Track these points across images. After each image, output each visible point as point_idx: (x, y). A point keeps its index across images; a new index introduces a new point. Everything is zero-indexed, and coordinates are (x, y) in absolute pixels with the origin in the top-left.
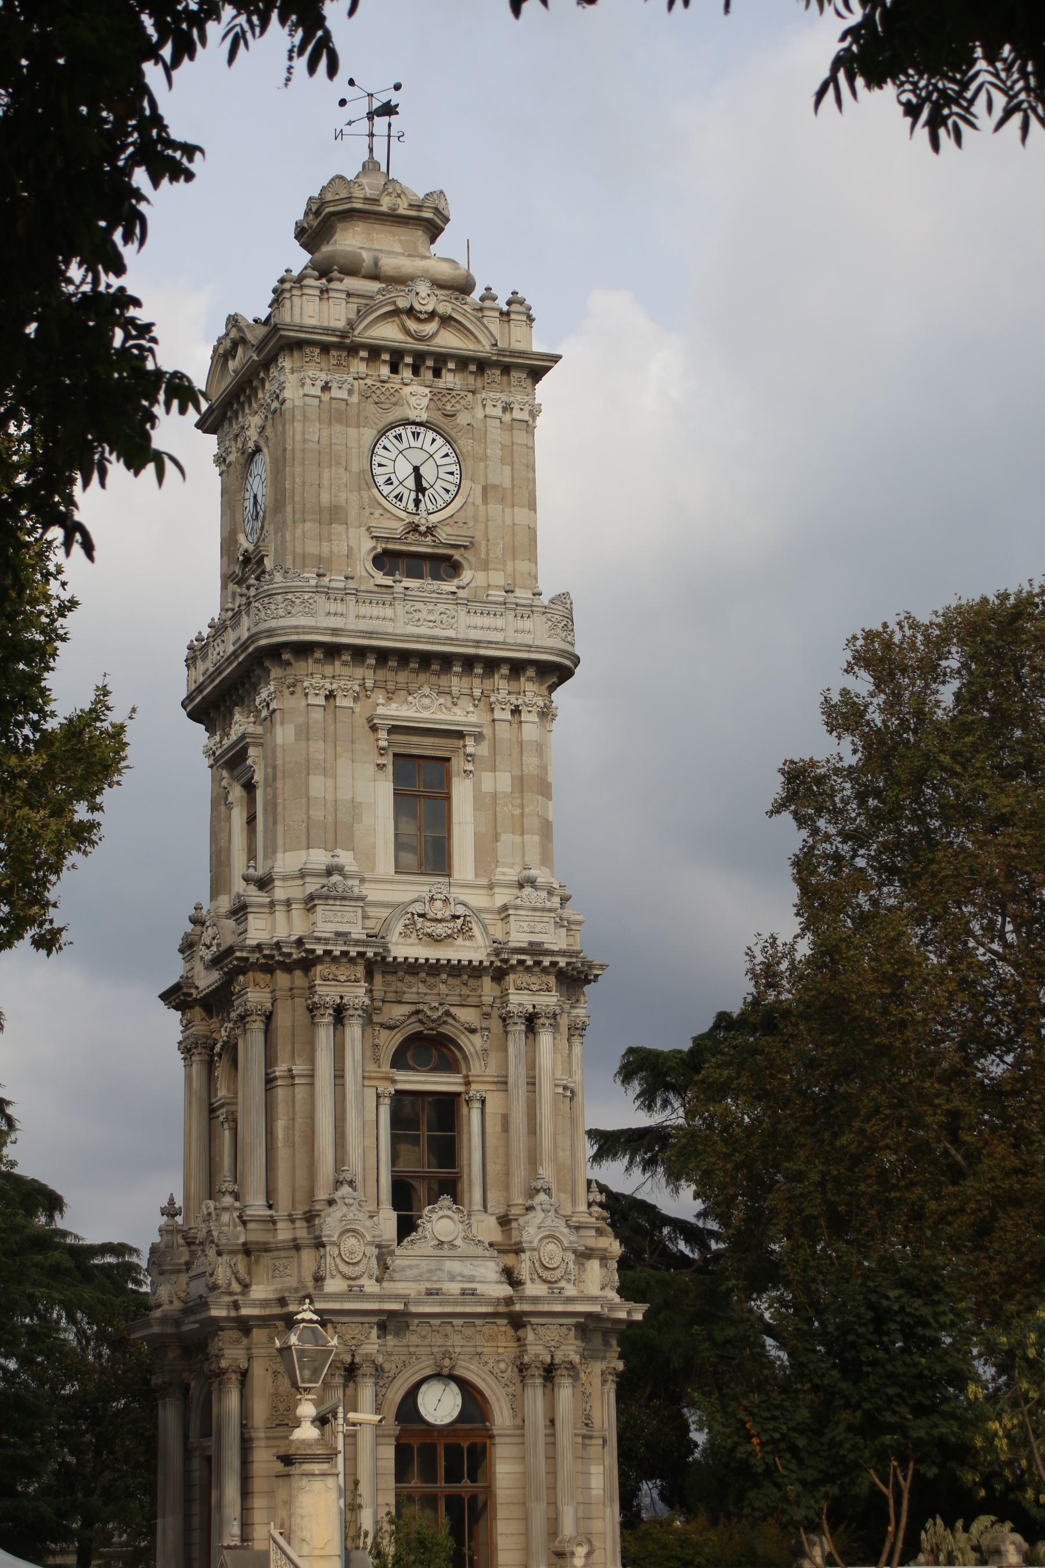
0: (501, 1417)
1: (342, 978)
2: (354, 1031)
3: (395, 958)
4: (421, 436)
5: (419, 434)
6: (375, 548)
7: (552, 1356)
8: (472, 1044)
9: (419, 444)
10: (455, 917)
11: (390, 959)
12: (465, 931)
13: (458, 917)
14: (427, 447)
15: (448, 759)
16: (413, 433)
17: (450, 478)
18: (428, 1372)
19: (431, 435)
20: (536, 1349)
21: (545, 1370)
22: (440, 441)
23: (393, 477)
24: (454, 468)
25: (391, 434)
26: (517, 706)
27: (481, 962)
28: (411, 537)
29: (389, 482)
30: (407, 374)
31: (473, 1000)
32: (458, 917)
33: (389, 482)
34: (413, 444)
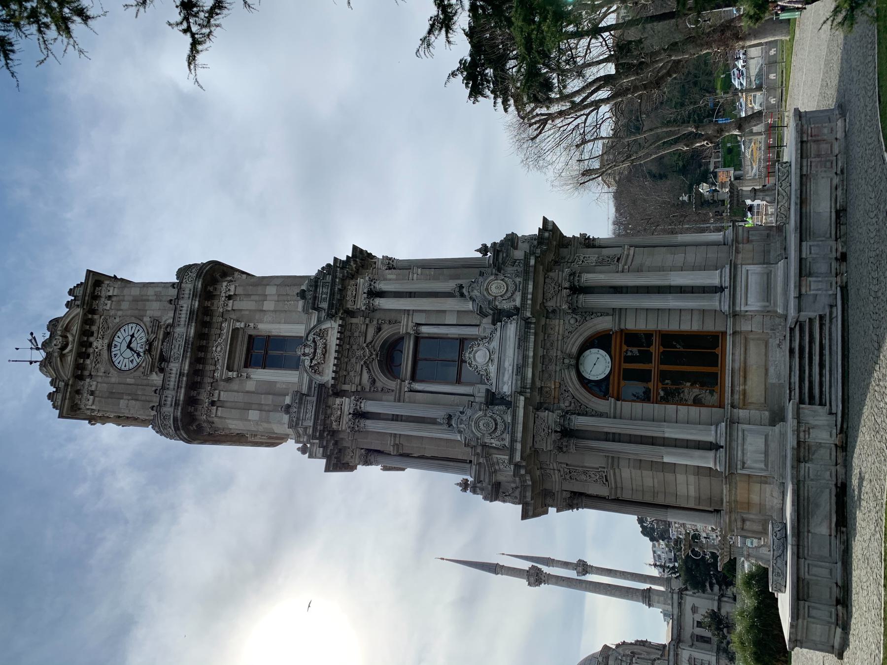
0: (604, 324)
1: (339, 413)
2: (369, 406)
3: (333, 378)
4: (116, 343)
5: (115, 345)
6: (156, 373)
7: (565, 288)
8: (387, 332)
9: (119, 344)
10: (314, 341)
11: (332, 382)
12: (322, 334)
13: (314, 338)
14: (120, 341)
15: (250, 336)
16: (115, 347)
17: (134, 328)
18: (573, 374)
19: (116, 339)
20: (560, 302)
21: (574, 293)
22: (119, 334)
23: (130, 359)
24: (130, 326)
25: (114, 359)
26: (226, 297)
27: (339, 325)
28: (154, 353)
29: (132, 361)
30: (91, 350)
31: (363, 327)
32: (314, 338)
33: (132, 361)
34: (118, 348)
